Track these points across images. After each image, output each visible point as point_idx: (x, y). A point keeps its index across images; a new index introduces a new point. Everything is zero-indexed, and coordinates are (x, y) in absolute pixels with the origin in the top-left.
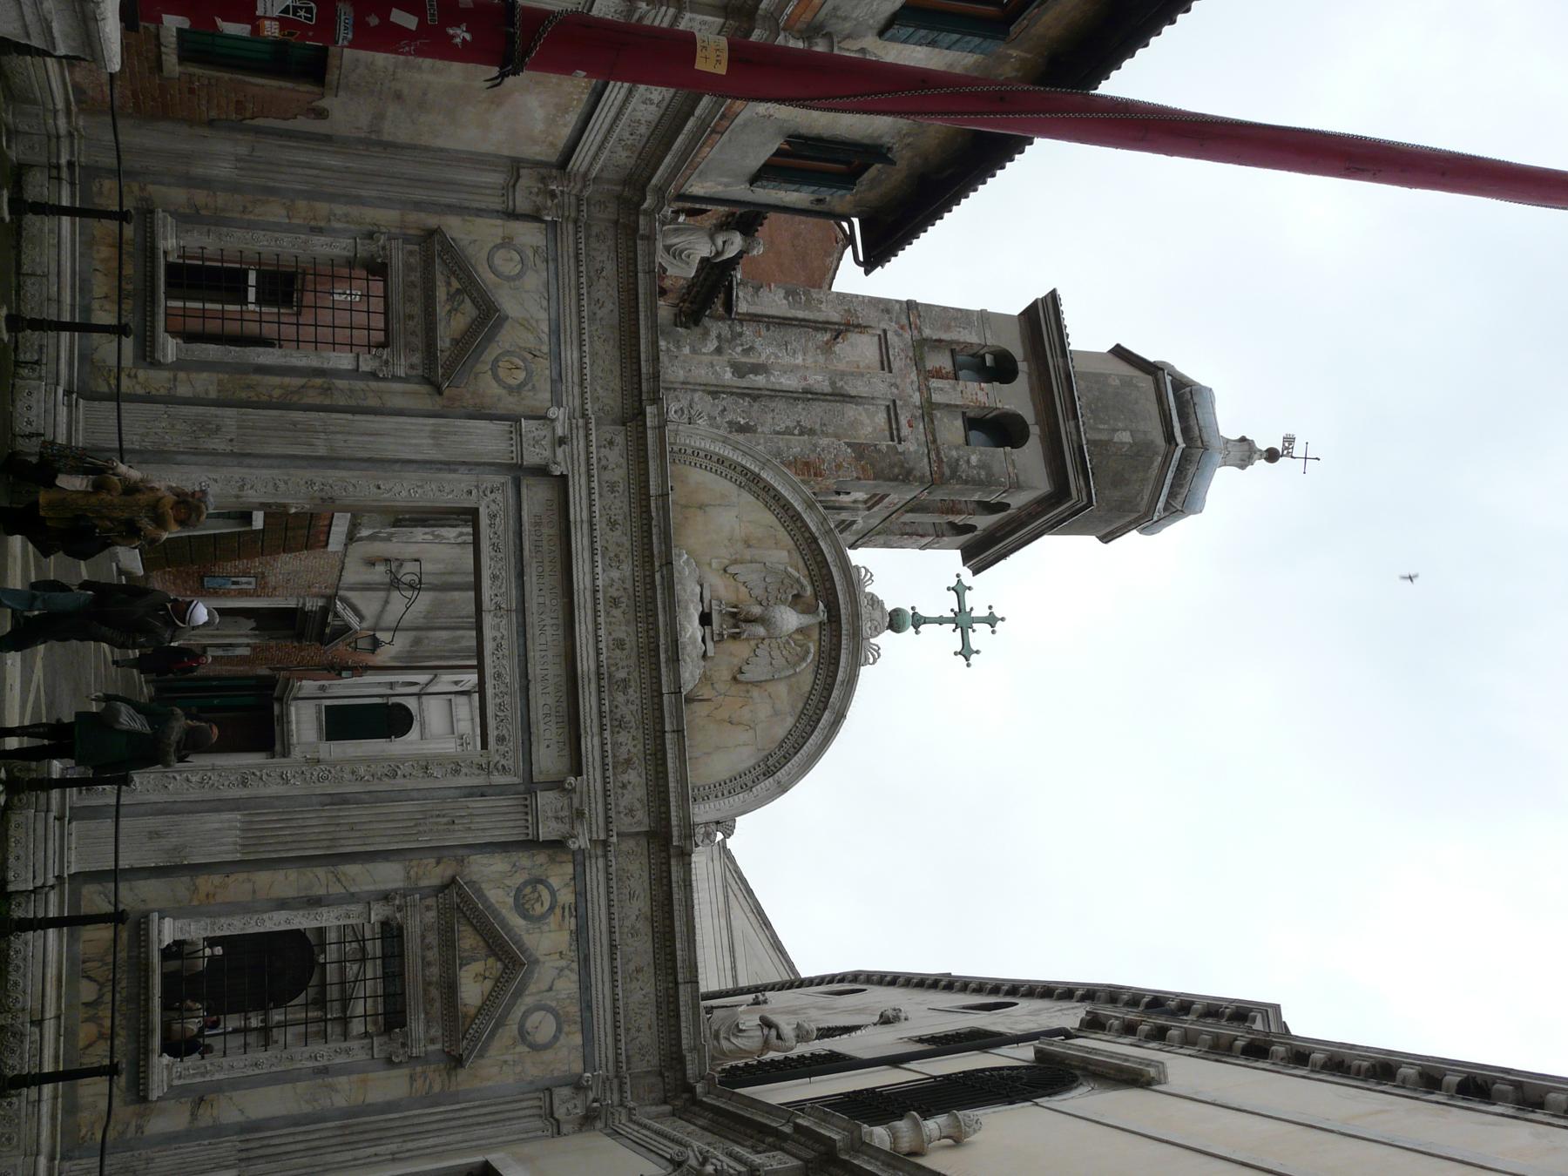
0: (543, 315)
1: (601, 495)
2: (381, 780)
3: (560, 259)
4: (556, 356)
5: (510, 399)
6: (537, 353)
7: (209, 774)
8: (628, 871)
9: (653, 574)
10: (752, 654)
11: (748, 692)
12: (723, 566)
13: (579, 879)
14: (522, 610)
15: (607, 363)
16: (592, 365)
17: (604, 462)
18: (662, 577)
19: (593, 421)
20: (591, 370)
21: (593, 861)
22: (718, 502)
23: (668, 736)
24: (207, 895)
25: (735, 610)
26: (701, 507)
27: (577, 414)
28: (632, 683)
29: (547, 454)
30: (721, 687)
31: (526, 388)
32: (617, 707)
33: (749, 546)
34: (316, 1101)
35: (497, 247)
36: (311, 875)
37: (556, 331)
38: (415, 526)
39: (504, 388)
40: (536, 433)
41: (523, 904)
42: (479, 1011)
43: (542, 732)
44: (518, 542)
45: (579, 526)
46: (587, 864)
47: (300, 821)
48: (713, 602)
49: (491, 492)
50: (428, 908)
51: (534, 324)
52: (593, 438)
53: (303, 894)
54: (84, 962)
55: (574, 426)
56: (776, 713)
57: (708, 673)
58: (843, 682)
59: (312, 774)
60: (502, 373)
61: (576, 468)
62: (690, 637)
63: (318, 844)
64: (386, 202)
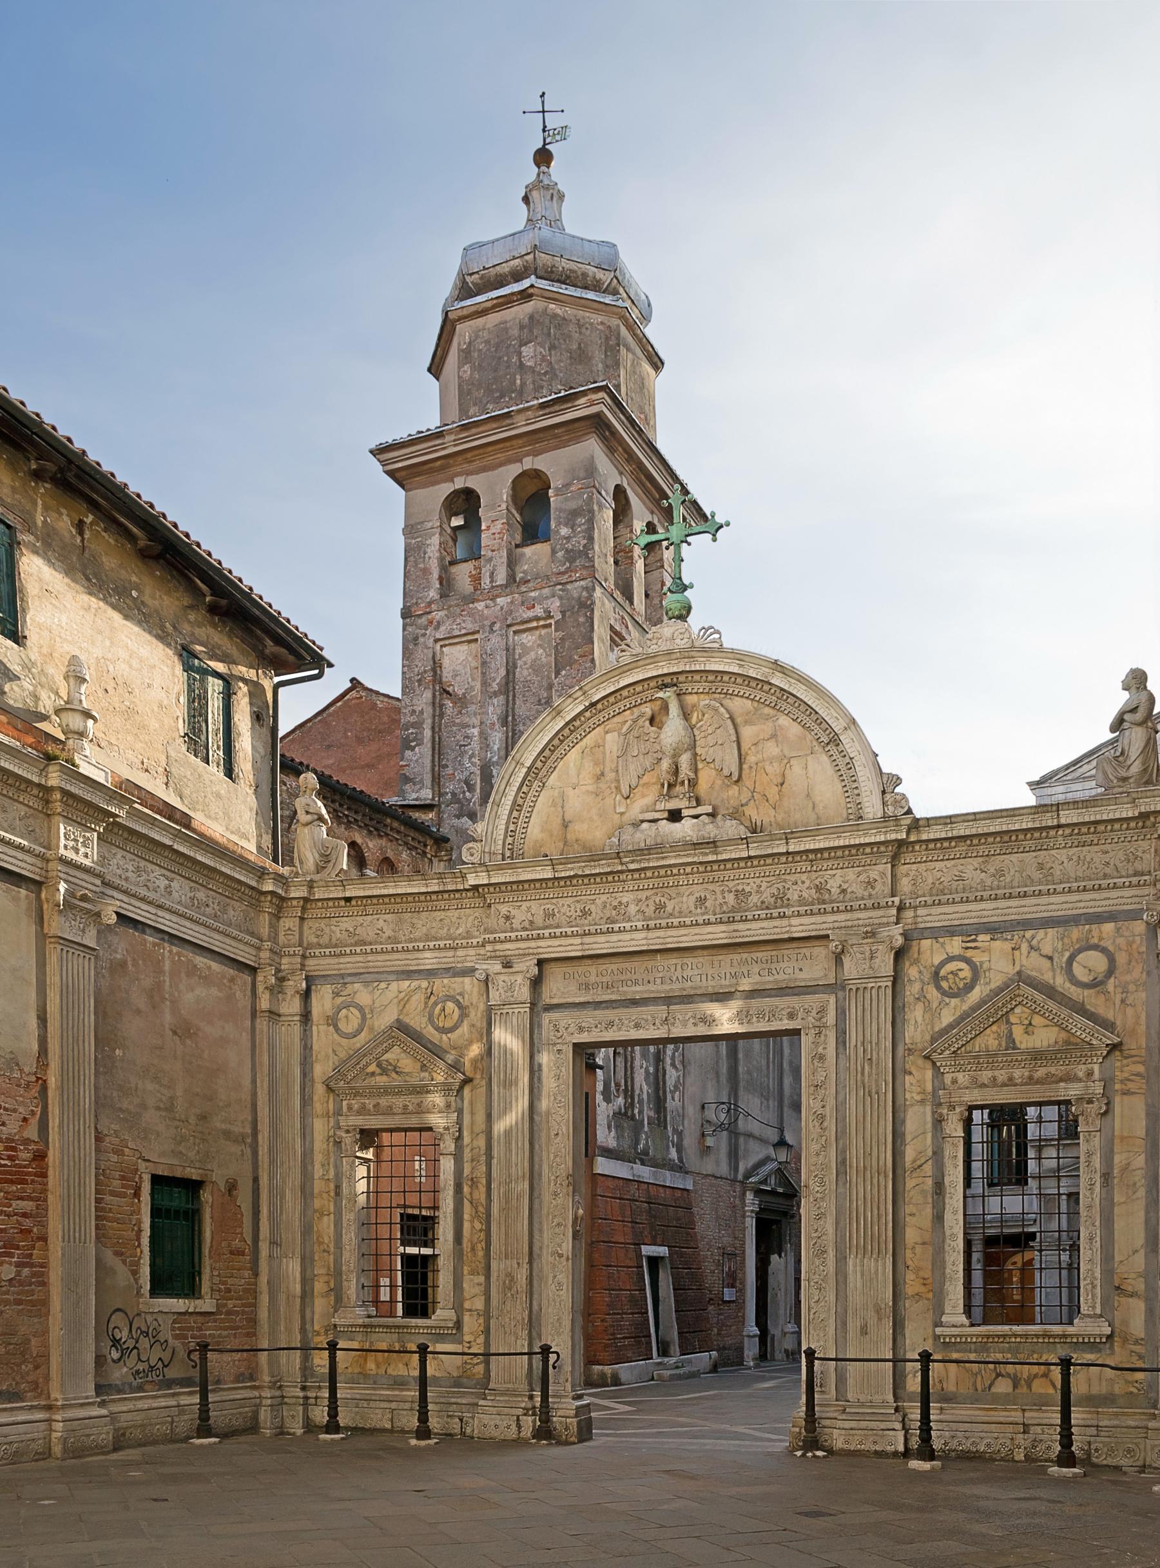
0: (394, 986)
1: (558, 927)
2: (826, 1128)
3: (342, 972)
4: (431, 973)
5: (472, 1014)
6: (429, 991)
7: (812, 1284)
8: (933, 883)
9: (629, 871)
10: (712, 765)
11: (751, 767)
12: (623, 800)
13: (936, 933)
14: (668, 1000)
15: (434, 925)
16: (437, 940)
17: (526, 924)
18: (633, 862)
19: (487, 936)
20: (441, 939)
21: (920, 919)
22: (560, 809)
23: (792, 849)
24: (925, 1284)
26: (565, 825)
27: (482, 952)
28: (740, 888)
29: (519, 978)
30: (745, 796)
31: (461, 1001)
32: (763, 902)
33: (602, 774)
34: (1135, 1184)
35: (337, 1029)
36: (911, 1194)
37: (408, 974)
38: (665, 1109)
39: (462, 1021)
40: (502, 991)
41: (958, 988)
42: (1064, 1029)
43: (786, 977)
44: (604, 1005)
45: (586, 947)
46: (922, 925)
47: (859, 1203)
48: (658, 808)
49: (558, 1031)
50: (954, 1081)
51: (403, 994)
52: (502, 936)
53: (930, 1200)
54: (977, 1390)
55: (493, 954)
56: (774, 736)
59: (818, 1192)
60: (449, 1024)
61: (531, 951)
63: (882, 1187)
64: (306, 1132)
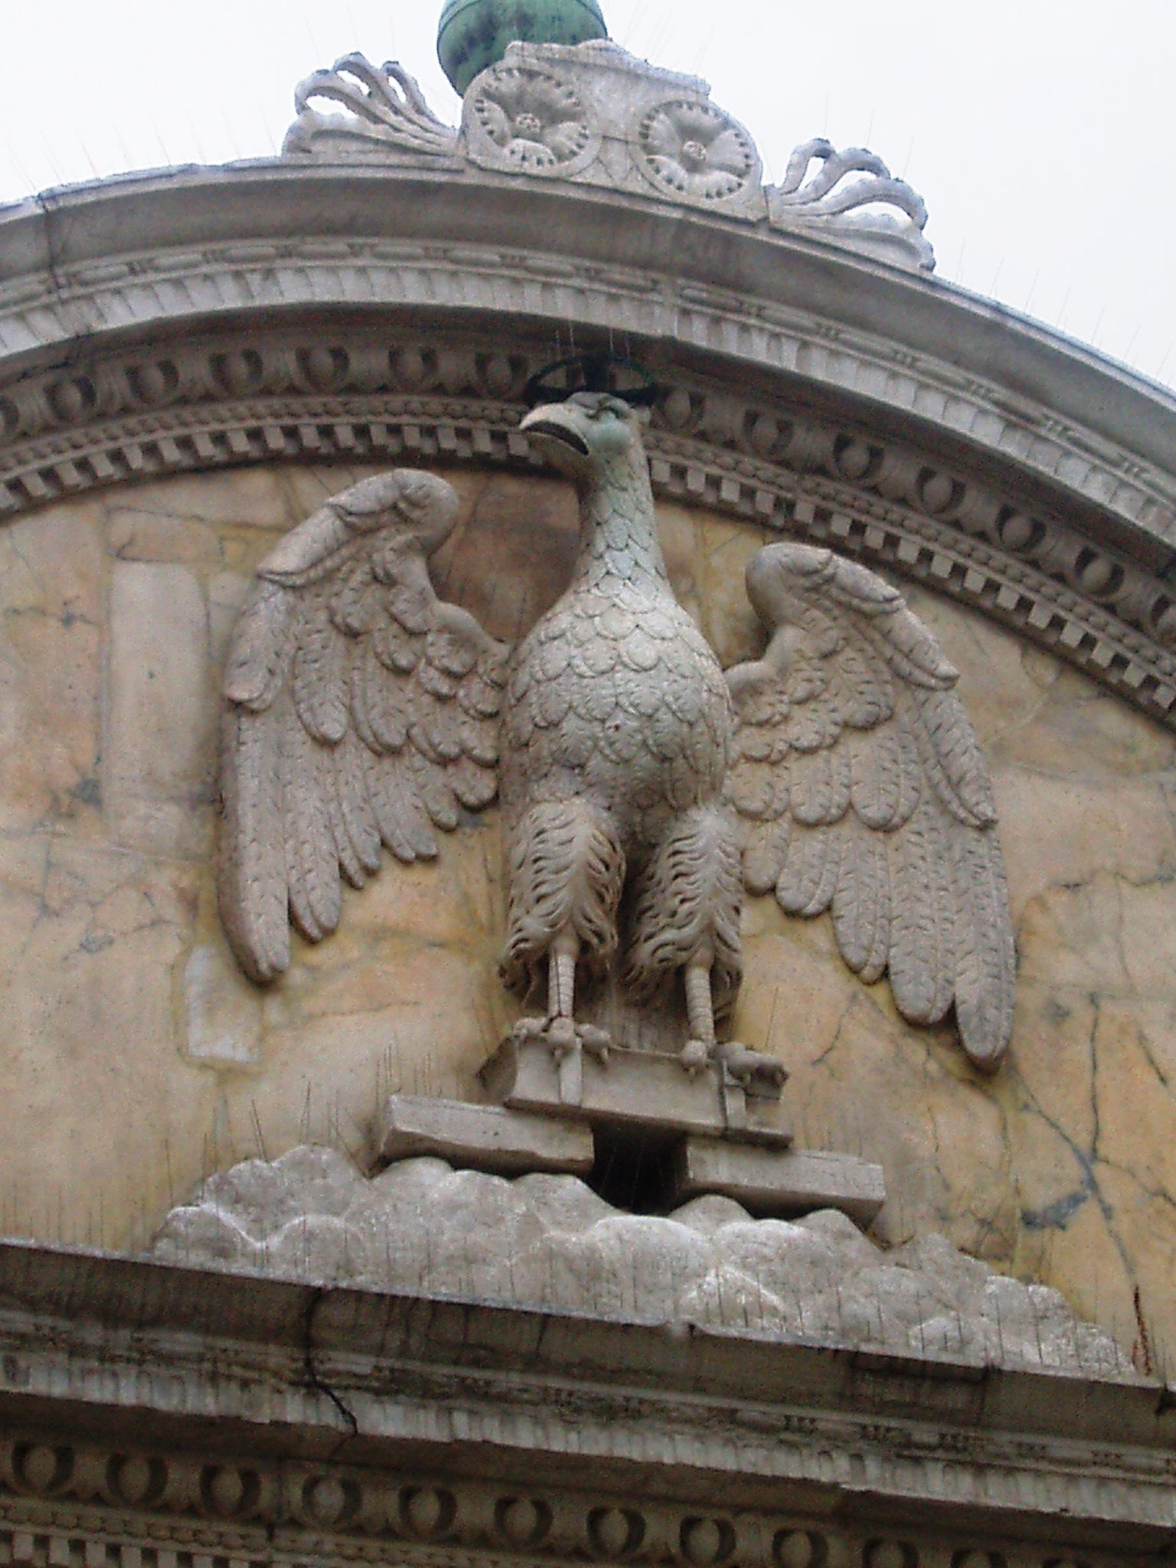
10: (818, 935)
11: (1059, 1014)
12: (235, 992)
25: (563, 971)
48: (529, 1084)
57: (967, 1233)
58: (1015, 421)
62: (775, 1282)
